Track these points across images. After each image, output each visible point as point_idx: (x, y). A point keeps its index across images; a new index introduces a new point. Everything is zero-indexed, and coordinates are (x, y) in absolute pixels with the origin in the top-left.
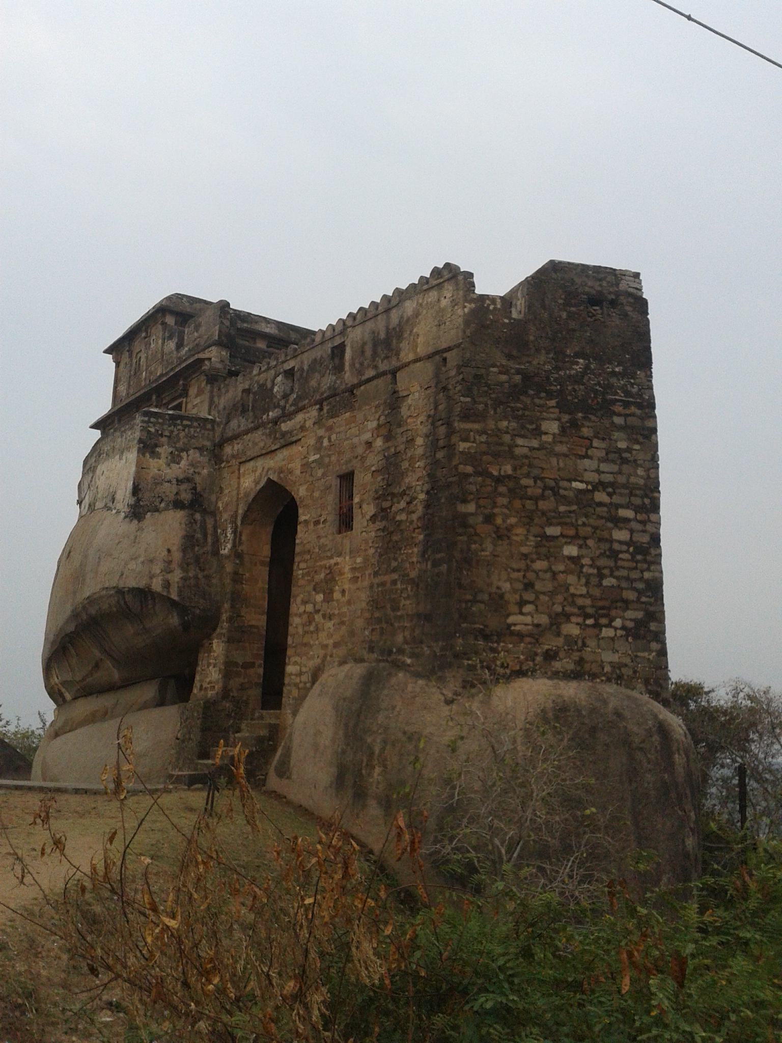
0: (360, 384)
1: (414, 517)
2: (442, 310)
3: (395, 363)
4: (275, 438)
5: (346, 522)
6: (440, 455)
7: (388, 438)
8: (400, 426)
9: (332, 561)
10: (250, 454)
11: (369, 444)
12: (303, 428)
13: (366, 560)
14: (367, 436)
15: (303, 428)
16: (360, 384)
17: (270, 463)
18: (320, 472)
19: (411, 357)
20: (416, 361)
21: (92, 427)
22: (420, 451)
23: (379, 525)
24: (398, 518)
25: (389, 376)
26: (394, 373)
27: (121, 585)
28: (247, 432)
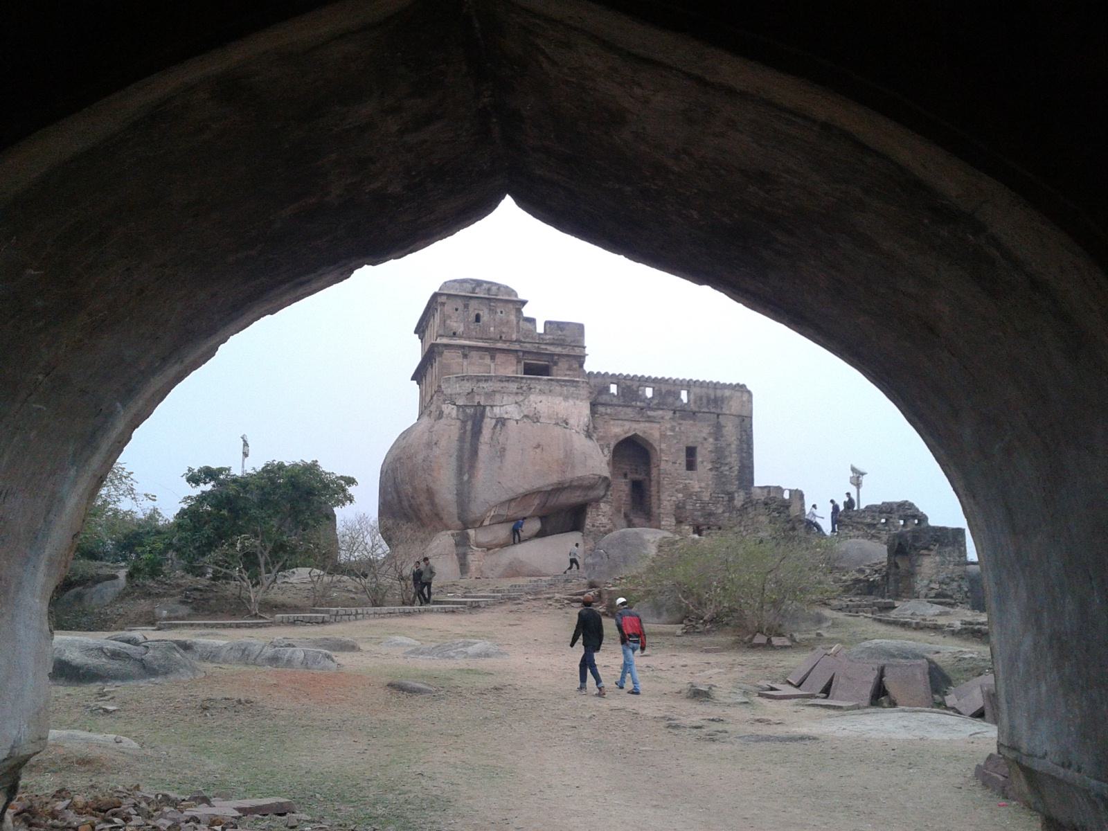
0: (700, 412)
1: (733, 474)
2: (744, 402)
3: (719, 411)
4: (642, 417)
5: (691, 465)
6: (744, 455)
7: (716, 439)
8: (722, 437)
9: (687, 482)
10: (620, 417)
11: (705, 439)
12: (662, 418)
13: (708, 485)
14: (704, 435)
15: (662, 418)
16: (697, 412)
17: (635, 426)
18: (675, 441)
19: (728, 412)
20: (731, 415)
21: (852, 466)
22: (734, 450)
23: (713, 473)
24: (725, 473)
25: (716, 416)
26: (718, 415)
27: (601, 474)
28: (619, 406)
